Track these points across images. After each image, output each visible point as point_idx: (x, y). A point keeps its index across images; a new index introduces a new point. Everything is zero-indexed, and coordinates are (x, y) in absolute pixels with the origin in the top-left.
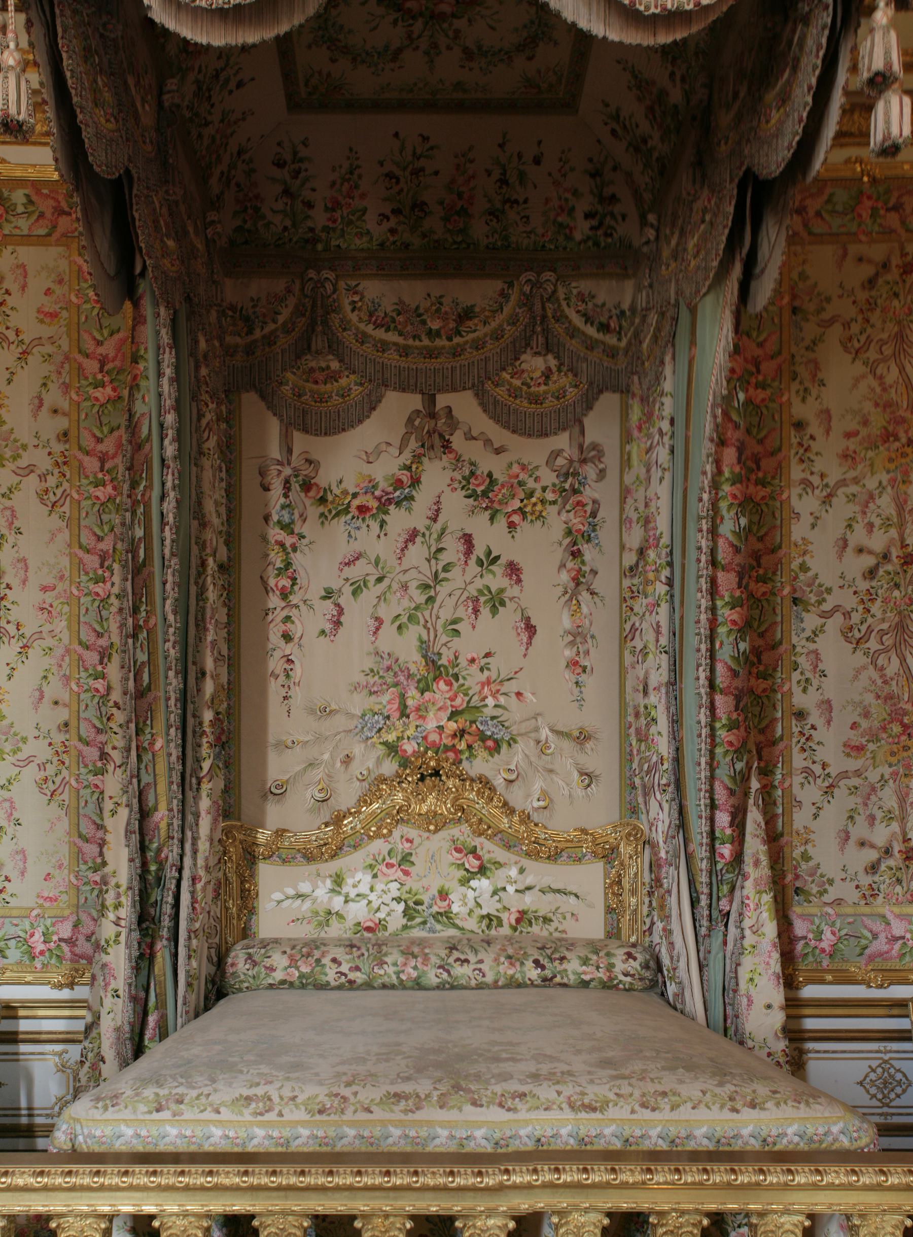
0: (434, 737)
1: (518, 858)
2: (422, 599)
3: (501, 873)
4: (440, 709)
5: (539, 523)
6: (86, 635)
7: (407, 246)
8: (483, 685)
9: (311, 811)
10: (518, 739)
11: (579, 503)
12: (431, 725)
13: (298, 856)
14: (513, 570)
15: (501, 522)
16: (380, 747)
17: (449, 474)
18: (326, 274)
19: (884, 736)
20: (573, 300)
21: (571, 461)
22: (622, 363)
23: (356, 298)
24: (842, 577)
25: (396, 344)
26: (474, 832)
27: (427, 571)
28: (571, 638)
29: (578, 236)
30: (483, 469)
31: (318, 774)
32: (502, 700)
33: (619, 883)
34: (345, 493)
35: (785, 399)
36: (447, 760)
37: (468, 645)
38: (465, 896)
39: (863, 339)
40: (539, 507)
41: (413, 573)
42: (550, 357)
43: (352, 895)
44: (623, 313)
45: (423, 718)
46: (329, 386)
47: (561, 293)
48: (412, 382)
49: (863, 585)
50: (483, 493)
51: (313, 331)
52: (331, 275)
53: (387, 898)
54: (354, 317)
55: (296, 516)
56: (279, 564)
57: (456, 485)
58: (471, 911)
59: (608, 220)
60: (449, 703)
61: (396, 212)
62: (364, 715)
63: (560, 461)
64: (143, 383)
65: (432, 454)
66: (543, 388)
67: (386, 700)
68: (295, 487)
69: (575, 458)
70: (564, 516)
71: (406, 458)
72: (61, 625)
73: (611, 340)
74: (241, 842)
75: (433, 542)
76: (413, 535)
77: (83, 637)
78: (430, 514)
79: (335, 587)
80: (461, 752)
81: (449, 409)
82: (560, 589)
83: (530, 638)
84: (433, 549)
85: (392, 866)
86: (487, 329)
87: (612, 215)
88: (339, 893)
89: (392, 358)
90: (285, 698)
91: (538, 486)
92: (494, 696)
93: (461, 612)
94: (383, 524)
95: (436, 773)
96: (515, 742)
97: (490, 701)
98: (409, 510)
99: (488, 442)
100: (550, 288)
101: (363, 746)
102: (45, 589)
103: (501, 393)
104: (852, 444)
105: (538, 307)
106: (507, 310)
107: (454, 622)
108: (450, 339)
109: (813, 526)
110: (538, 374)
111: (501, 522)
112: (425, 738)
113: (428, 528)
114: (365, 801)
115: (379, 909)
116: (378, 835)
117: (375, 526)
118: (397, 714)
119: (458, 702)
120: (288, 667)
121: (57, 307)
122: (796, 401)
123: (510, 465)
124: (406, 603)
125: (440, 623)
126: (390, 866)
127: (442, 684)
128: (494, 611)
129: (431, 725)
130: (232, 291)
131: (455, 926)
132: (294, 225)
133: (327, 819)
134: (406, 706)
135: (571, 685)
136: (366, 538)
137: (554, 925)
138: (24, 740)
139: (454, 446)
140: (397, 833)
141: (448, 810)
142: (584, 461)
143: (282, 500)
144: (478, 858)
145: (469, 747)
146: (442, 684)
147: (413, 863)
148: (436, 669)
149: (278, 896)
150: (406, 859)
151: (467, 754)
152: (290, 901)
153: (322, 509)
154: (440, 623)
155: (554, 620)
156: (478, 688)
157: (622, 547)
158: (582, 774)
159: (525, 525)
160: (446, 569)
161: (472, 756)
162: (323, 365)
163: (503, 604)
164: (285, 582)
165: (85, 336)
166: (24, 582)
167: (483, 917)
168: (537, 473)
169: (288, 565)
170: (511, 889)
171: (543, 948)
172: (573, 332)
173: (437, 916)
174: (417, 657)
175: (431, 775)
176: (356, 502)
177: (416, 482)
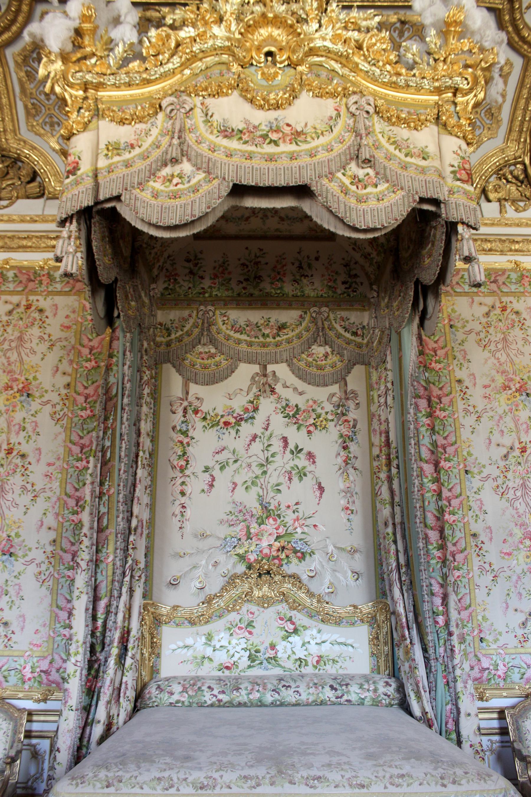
0: (266, 551)
1: (317, 624)
2: (259, 472)
3: (308, 632)
4: (270, 534)
5: (324, 431)
6: (70, 490)
7: (251, 295)
8: (295, 521)
9: (193, 594)
10: (316, 552)
11: (346, 421)
12: (264, 544)
13: (186, 622)
14: (311, 456)
15: (304, 430)
16: (236, 557)
17: (275, 405)
18: (209, 307)
19: (522, 546)
20: (338, 320)
21: (341, 399)
22: (365, 350)
23: (225, 318)
24: (490, 459)
25: (245, 340)
26: (290, 608)
27: (262, 457)
28: (344, 494)
29: (339, 291)
30: (292, 403)
31: (199, 572)
32: (306, 529)
33: (377, 638)
34: (217, 415)
35: (451, 368)
36: (274, 565)
37: (286, 498)
38: (285, 647)
39: (487, 340)
40: (324, 422)
41: (254, 458)
42: (327, 347)
43: (218, 647)
44: (364, 327)
45: (260, 540)
46: (209, 361)
47: (332, 316)
48: (254, 358)
49: (502, 464)
50: (293, 414)
51: (202, 334)
52: (212, 308)
53: (238, 649)
54: (224, 328)
55: (190, 427)
56: (180, 453)
57: (278, 411)
58: (289, 656)
59: (354, 285)
60: (275, 531)
61: (247, 280)
62: (226, 538)
63: (335, 399)
64: (115, 368)
65: (265, 395)
66: (324, 362)
67: (239, 530)
68: (190, 412)
69: (343, 397)
70: (338, 426)
71: (251, 397)
72: (56, 485)
73: (359, 340)
74: (152, 613)
75: (265, 441)
76: (254, 438)
77: (68, 491)
78: (264, 426)
79: (210, 465)
80: (282, 559)
81: (274, 373)
82: (337, 467)
83: (321, 494)
84: (266, 445)
85: (242, 628)
86: (294, 333)
87: (356, 282)
88: (210, 645)
89: (243, 347)
90: (180, 528)
91: (323, 412)
92: (301, 526)
93: (282, 480)
94: (238, 431)
95: (268, 573)
96: (314, 553)
97: (299, 530)
98: (252, 424)
99: (295, 389)
100: (326, 315)
101: (225, 556)
102: (49, 465)
103: (302, 364)
104: (488, 391)
105: (320, 324)
106: (304, 324)
107: (278, 485)
108: (274, 338)
109: (473, 432)
110: (321, 355)
111: (304, 430)
112: (261, 552)
113: (263, 434)
114: (226, 589)
115: (233, 655)
116: (233, 610)
117: (233, 432)
118: (245, 538)
119: (280, 531)
120: (183, 510)
121: (71, 324)
122: (457, 369)
123: (308, 401)
124: (251, 475)
125: (270, 485)
126: (240, 628)
127: (271, 520)
128: (301, 479)
129: (264, 544)
130: (161, 316)
131: (279, 665)
132: (194, 287)
133: (202, 600)
134: (250, 533)
135: (345, 520)
136: (229, 438)
137: (340, 664)
138: (30, 549)
139: (277, 391)
140: (244, 609)
141: (275, 595)
142: (347, 399)
143: (183, 419)
144: (293, 623)
145: (287, 556)
146: (271, 520)
147: (254, 627)
148: (268, 512)
149: (173, 646)
150: (250, 624)
151: (286, 561)
152: (180, 650)
153: (204, 423)
154: (270, 485)
155: (335, 484)
156: (291, 522)
157: (372, 445)
158: (353, 572)
159: (317, 432)
160: (273, 455)
161: (289, 562)
162: (207, 350)
163: (305, 475)
164: (183, 463)
165: (84, 337)
166: (38, 461)
167: (296, 660)
168: (323, 405)
169: (185, 453)
170: (313, 642)
171: (335, 679)
172: (339, 336)
173: (269, 659)
174: (257, 505)
175: (265, 574)
176: (223, 420)
177: (256, 409)
